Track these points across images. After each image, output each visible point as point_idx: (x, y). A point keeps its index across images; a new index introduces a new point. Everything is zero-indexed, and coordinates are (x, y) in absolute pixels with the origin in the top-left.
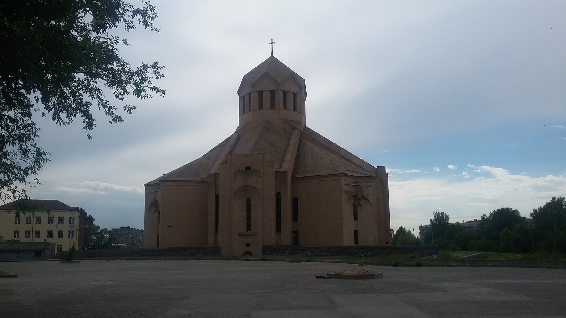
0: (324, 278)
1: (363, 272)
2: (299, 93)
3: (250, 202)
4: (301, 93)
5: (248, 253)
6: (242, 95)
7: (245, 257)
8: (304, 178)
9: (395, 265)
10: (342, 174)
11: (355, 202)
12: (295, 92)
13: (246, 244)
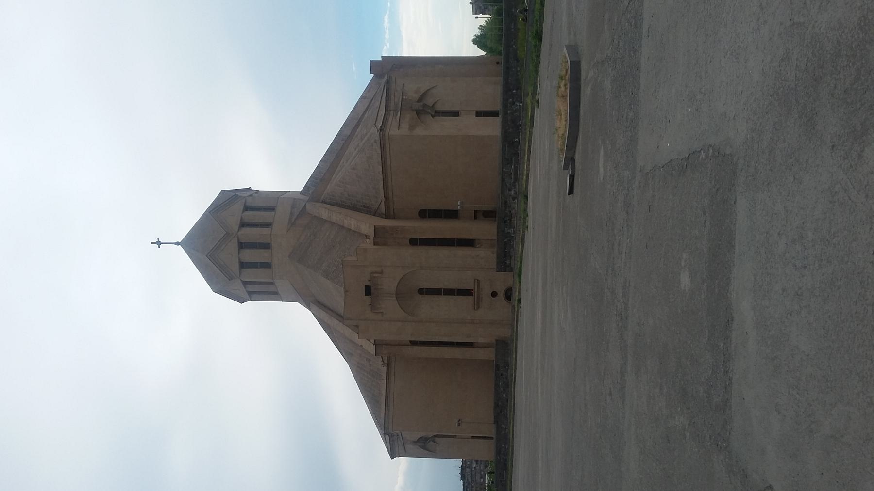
0: (572, 177)
1: (563, 88)
2: (244, 201)
4: (245, 197)
5: (508, 295)
6: (247, 296)
7: (515, 296)
9: (540, 39)
10: (381, 133)
11: (430, 113)
12: (242, 208)
13: (493, 298)
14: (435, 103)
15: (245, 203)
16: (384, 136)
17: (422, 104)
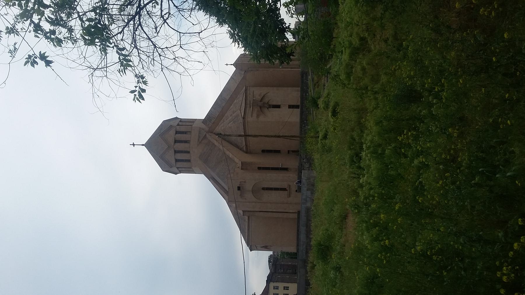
8: (246, 145)
10: (244, 120)
12: (175, 132)
14: (269, 101)
15: (176, 130)
16: (245, 121)
17: (262, 103)
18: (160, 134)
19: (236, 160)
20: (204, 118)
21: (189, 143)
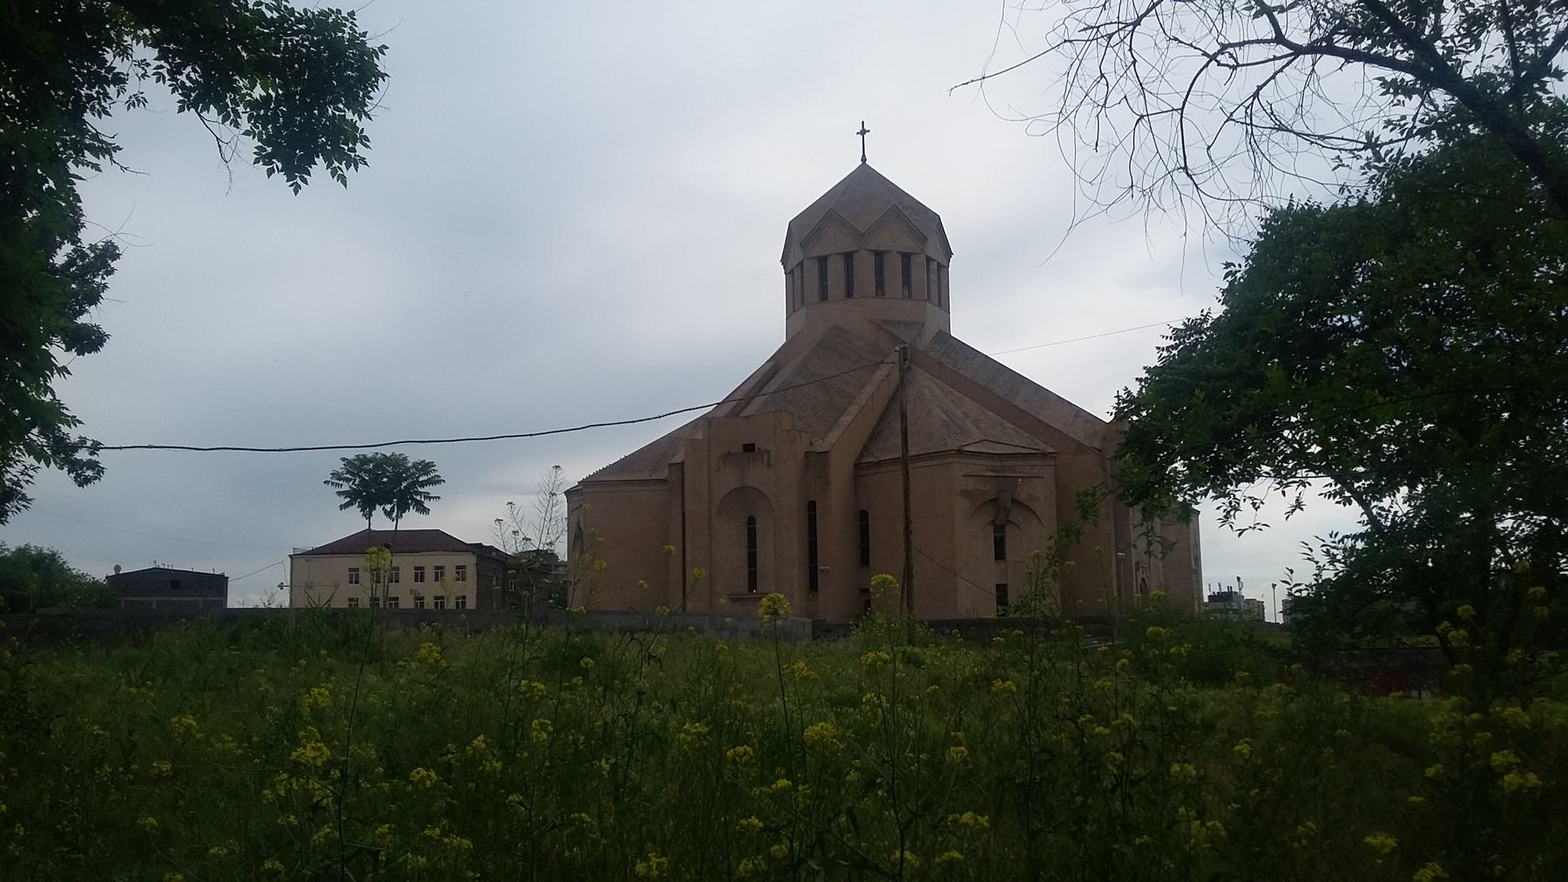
2: (919, 251)
3: (755, 524)
6: (789, 270)
8: (879, 463)
14: (1014, 524)
15: (914, 254)
16: (951, 456)
17: (1009, 505)
18: (900, 207)
19: (833, 436)
20: (955, 332)
21: (877, 294)
